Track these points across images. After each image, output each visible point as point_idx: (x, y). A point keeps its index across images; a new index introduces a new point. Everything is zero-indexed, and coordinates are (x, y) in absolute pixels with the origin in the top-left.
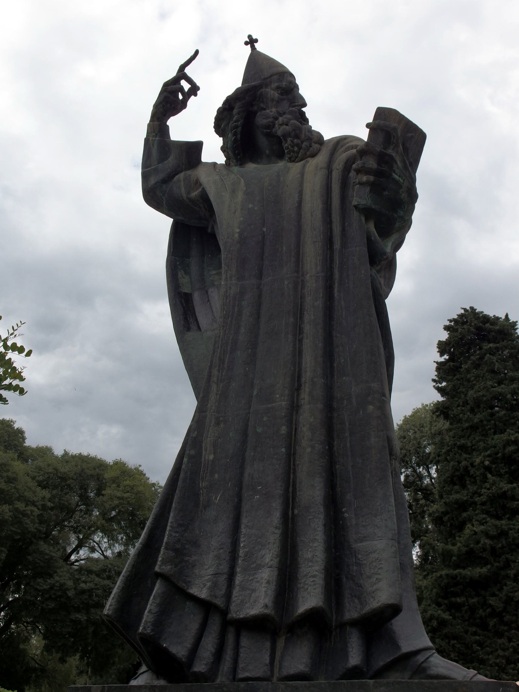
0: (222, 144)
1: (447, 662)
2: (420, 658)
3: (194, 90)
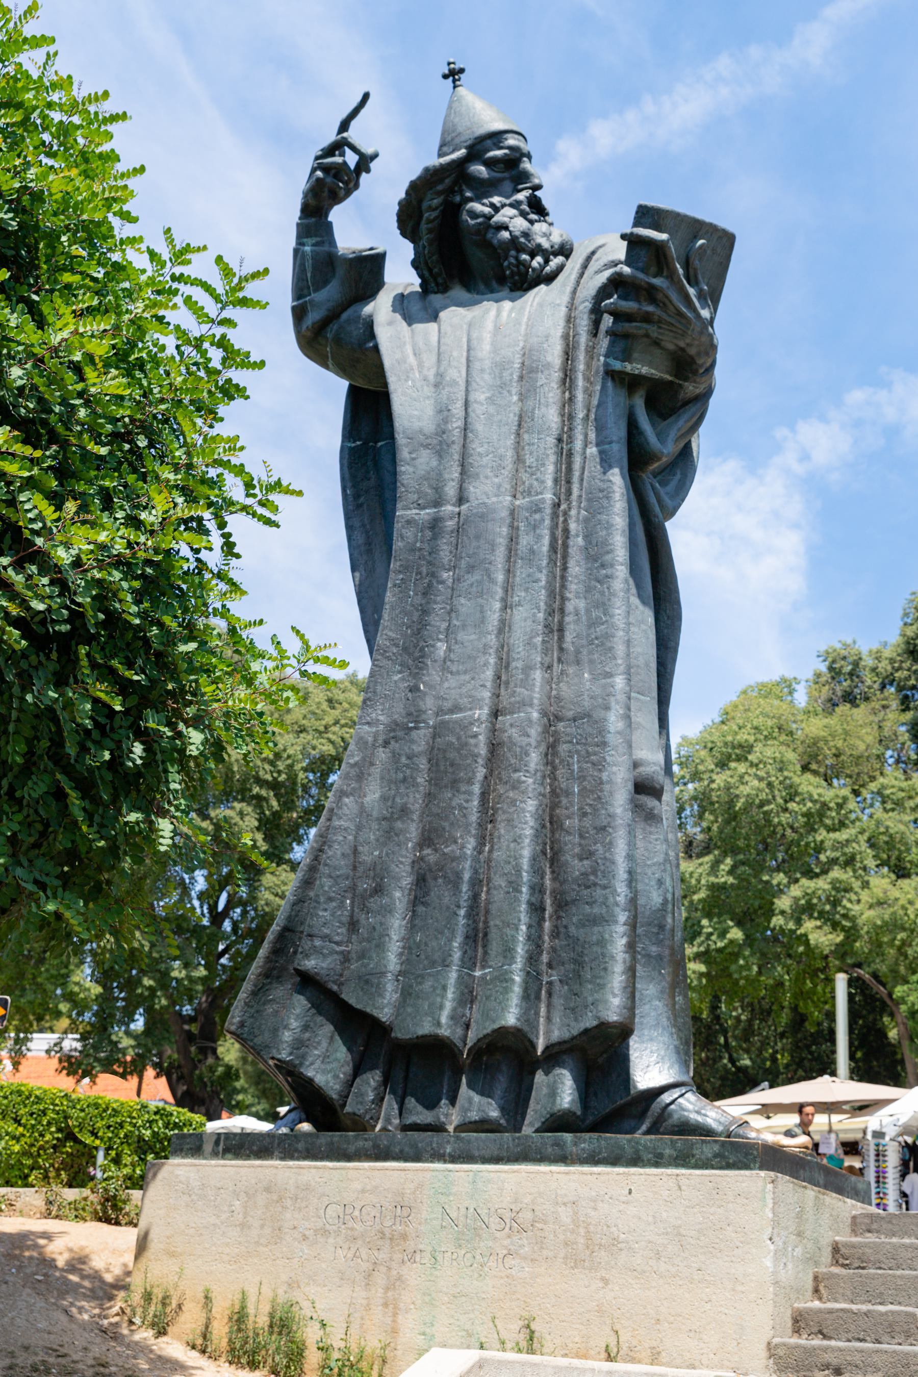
0: (412, 256)
1: (324, 1167)
2: (667, 1098)
3: (365, 162)
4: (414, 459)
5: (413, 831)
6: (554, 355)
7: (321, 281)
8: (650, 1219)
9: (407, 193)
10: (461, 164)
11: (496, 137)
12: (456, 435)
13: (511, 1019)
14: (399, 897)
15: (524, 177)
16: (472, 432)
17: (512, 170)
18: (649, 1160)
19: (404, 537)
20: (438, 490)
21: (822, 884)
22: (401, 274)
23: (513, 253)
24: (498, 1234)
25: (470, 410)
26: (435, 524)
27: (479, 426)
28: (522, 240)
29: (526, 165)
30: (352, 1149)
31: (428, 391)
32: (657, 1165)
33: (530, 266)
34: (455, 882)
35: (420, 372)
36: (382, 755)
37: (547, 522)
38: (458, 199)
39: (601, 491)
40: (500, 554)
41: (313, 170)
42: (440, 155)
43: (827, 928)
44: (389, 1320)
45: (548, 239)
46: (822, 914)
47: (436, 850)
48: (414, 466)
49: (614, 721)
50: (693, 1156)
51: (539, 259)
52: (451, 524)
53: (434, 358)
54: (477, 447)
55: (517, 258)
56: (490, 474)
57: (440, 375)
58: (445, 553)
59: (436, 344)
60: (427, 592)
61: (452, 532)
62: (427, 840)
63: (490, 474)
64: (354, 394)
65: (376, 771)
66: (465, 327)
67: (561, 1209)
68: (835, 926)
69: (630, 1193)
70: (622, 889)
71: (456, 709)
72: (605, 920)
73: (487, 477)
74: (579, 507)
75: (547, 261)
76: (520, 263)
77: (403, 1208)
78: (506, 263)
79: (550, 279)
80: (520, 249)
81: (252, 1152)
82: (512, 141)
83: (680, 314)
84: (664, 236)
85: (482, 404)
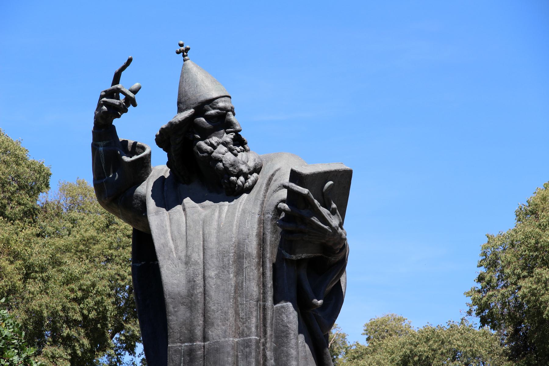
4: (176, 312)
6: (253, 247)
10: (190, 120)
11: (211, 102)
12: (200, 297)
17: (222, 121)
20: (191, 331)
22: (160, 167)
25: (206, 282)
26: (191, 352)
27: (212, 293)
28: (231, 169)
29: (232, 118)
31: (182, 267)
33: (237, 183)
35: (176, 253)
37: (253, 354)
45: (246, 165)
48: (177, 316)
51: (242, 178)
52: (200, 353)
53: (184, 244)
54: (212, 306)
56: (220, 323)
57: (188, 257)
59: (185, 233)
61: (201, 358)
63: (220, 323)
64: (135, 232)
73: (218, 325)
74: (271, 341)
75: (246, 179)
79: (248, 190)
82: (221, 104)
84: (305, 191)
85: (213, 279)
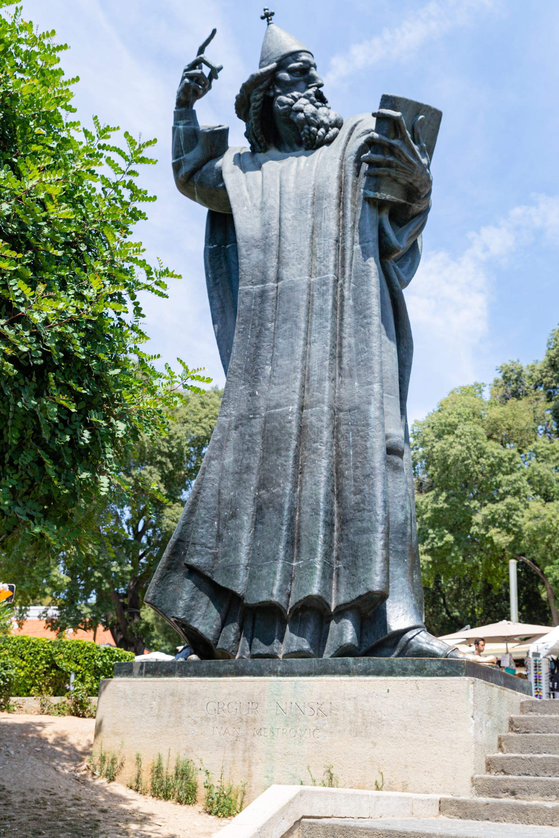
0: (245, 130)
2: (409, 635)
4: (249, 255)
5: (254, 480)
6: (333, 189)
7: (189, 148)
8: (401, 707)
9: (241, 91)
11: (294, 55)
12: (274, 240)
13: (315, 591)
14: (246, 519)
15: (311, 80)
16: (284, 237)
17: (305, 75)
18: (399, 672)
19: (244, 302)
20: (264, 273)
21: (500, 507)
22: (238, 141)
23: (306, 126)
24: (310, 718)
25: (282, 224)
26: (263, 294)
27: (288, 233)
28: (312, 118)
29: (313, 72)
30: (222, 669)
31: (257, 212)
32: (404, 675)
33: (317, 134)
34: (279, 510)
35: (251, 201)
36: (234, 435)
37: (331, 291)
38: (272, 94)
39: (363, 271)
40: (303, 311)
41: (183, 78)
42: (261, 67)
43: (504, 533)
44: (246, 769)
45: (328, 118)
46: (501, 525)
47: (268, 491)
48: (249, 259)
49: (373, 411)
50: (426, 669)
51: (322, 130)
52: (272, 294)
53: (260, 193)
54: (287, 247)
55: (309, 130)
56: (296, 263)
57: (263, 203)
58: (269, 312)
59: (260, 184)
60: (259, 336)
61: (273, 299)
62: (262, 485)
63: (296, 263)
64: (212, 216)
65: (231, 444)
66: (278, 173)
67: (347, 702)
68: (509, 531)
69: (388, 691)
70: (380, 512)
71: (278, 406)
72: (369, 531)
73: (293, 265)
74: (350, 282)
75: (327, 131)
76: (311, 132)
77: (253, 704)
78: (302, 133)
79: (329, 142)
80: (311, 124)
81: (162, 673)
82: (304, 57)
83: (409, 162)
84: (398, 114)
85: (290, 220)
